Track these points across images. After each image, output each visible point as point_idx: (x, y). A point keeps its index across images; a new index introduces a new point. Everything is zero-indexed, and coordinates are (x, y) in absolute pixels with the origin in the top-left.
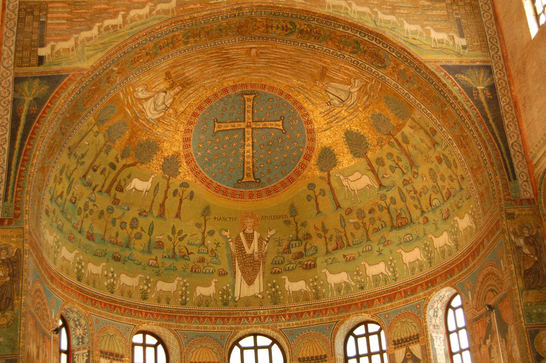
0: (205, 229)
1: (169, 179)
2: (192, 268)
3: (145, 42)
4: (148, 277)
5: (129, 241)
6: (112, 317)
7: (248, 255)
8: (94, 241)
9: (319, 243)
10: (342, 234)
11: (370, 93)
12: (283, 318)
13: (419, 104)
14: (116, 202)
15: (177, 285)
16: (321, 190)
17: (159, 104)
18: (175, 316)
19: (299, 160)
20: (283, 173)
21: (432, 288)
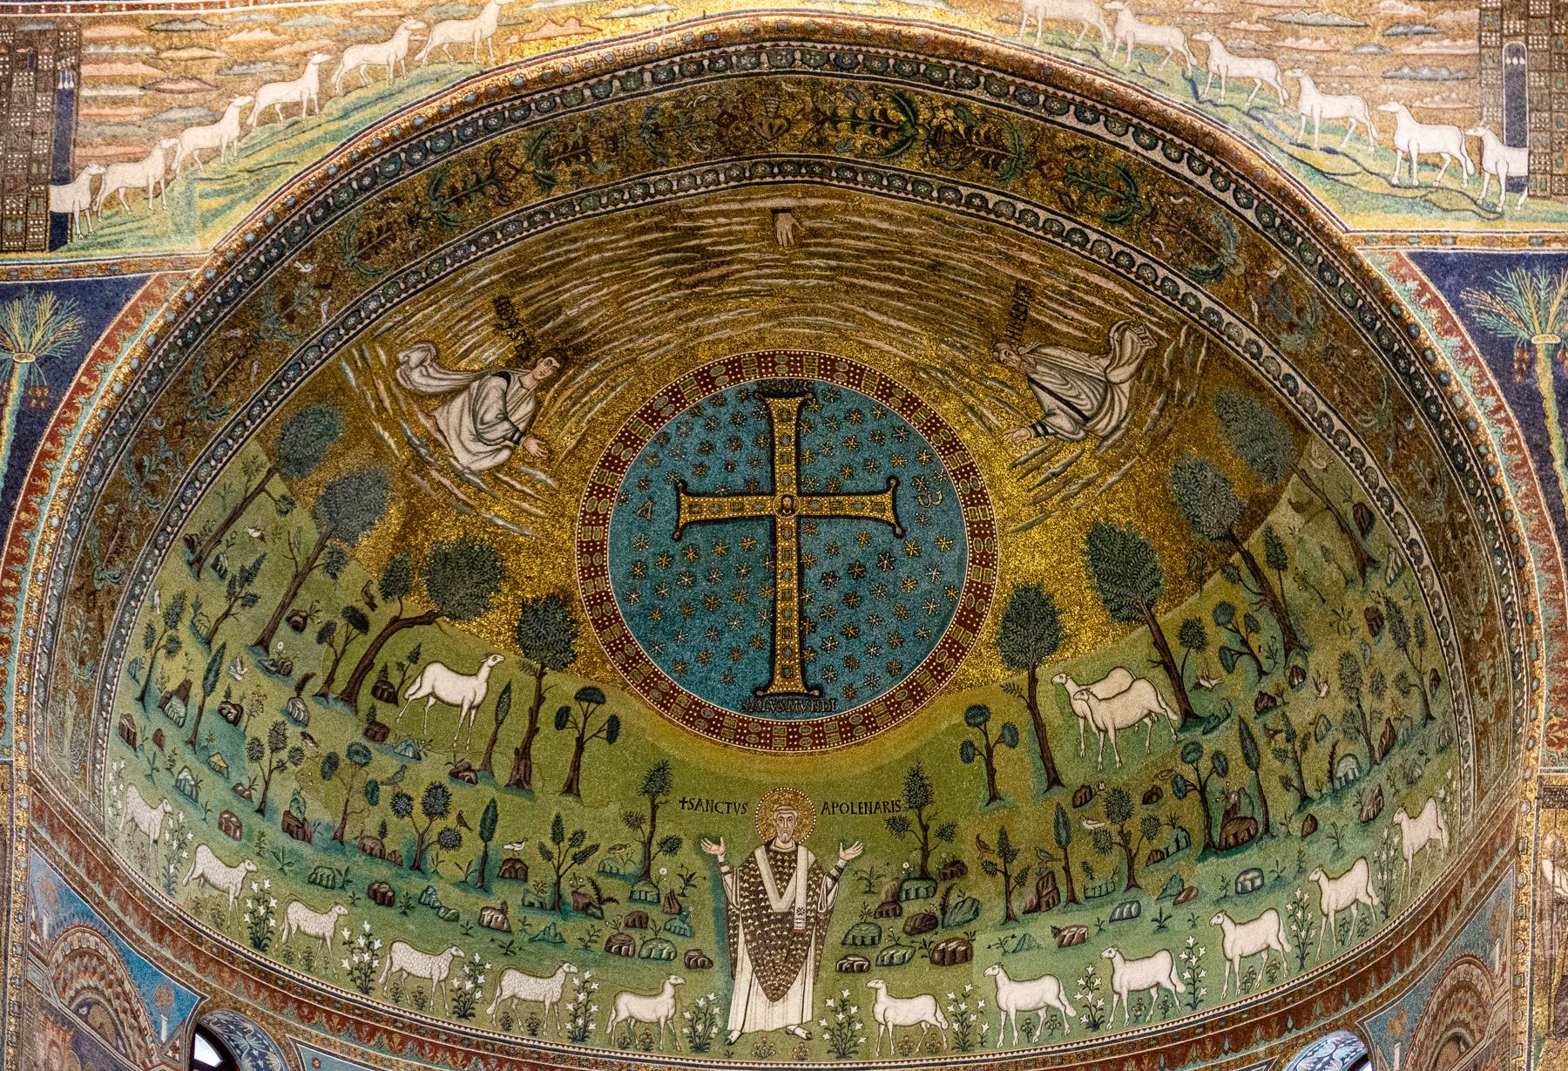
0: (652, 833)
1: (543, 674)
2: (609, 940)
7: (776, 914)
11: (1173, 385)
20: (894, 671)
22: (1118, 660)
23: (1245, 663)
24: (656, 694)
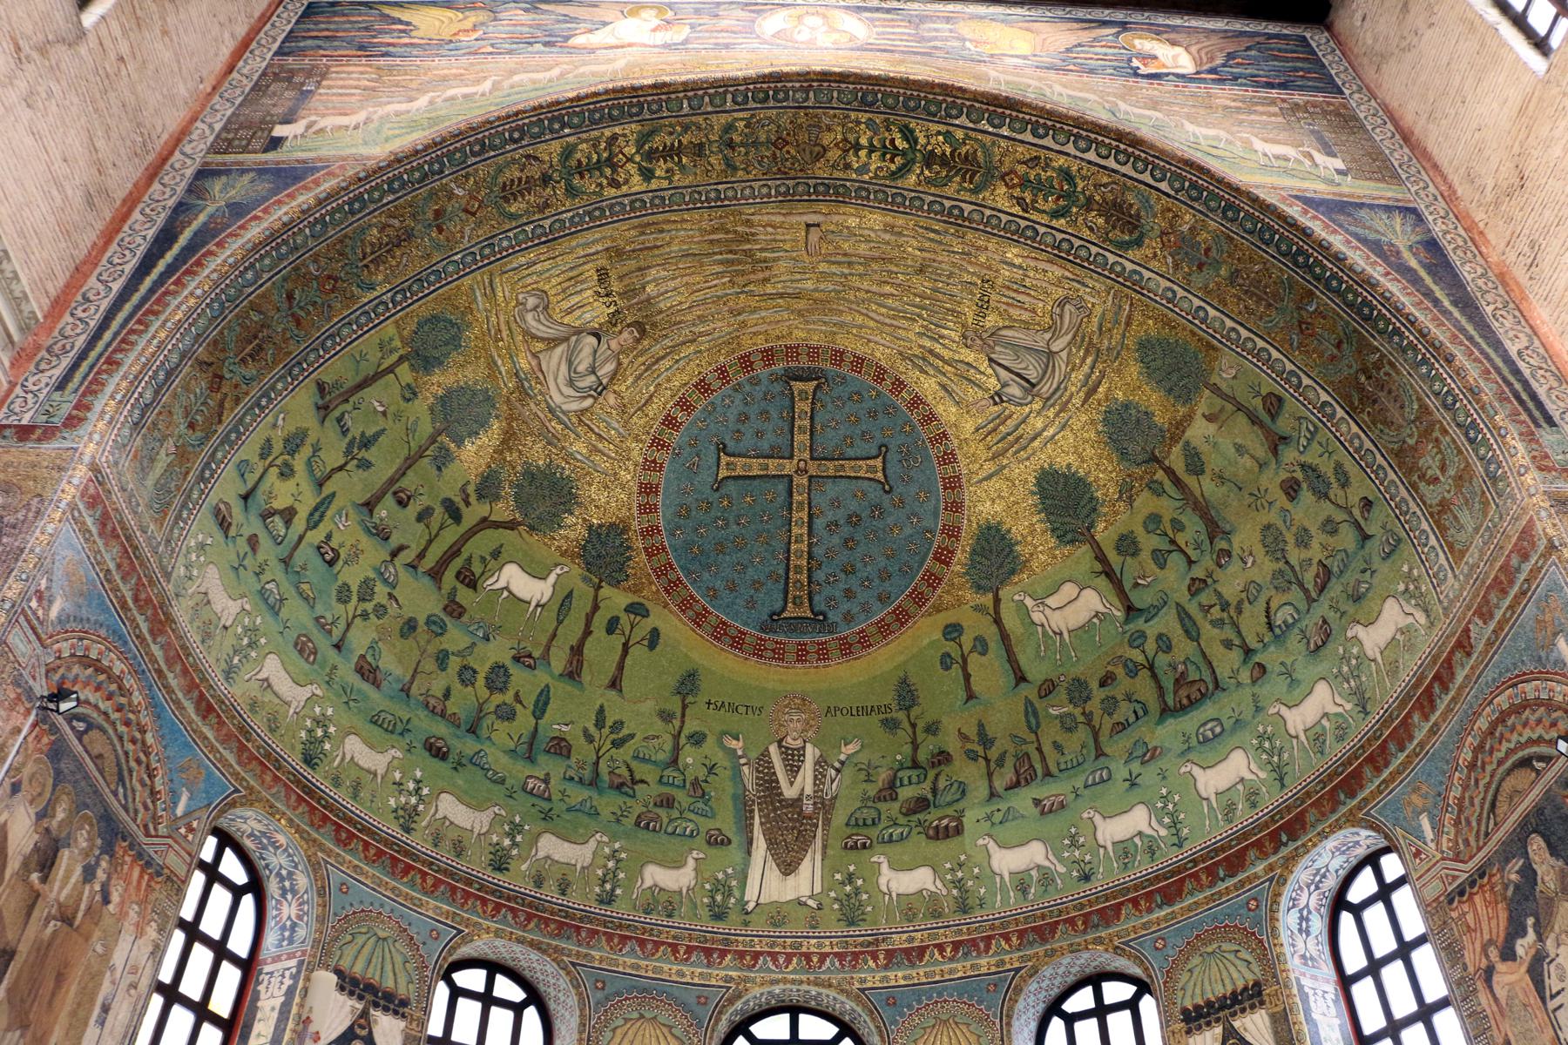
1: (600, 587)
3: (536, 130)
4: (517, 819)
5: (480, 719)
6: (393, 889)
8: (378, 687)
9: (971, 773)
10: (1031, 749)
12: (871, 963)
13: (1234, 329)
14: (455, 609)
15: (594, 853)
16: (976, 639)
17: (581, 368)
18: (578, 929)
19: (921, 564)
20: (883, 599)
21: (1292, 846)
22: (1066, 576)
23: (1176, 559)
24: (691, 613)
